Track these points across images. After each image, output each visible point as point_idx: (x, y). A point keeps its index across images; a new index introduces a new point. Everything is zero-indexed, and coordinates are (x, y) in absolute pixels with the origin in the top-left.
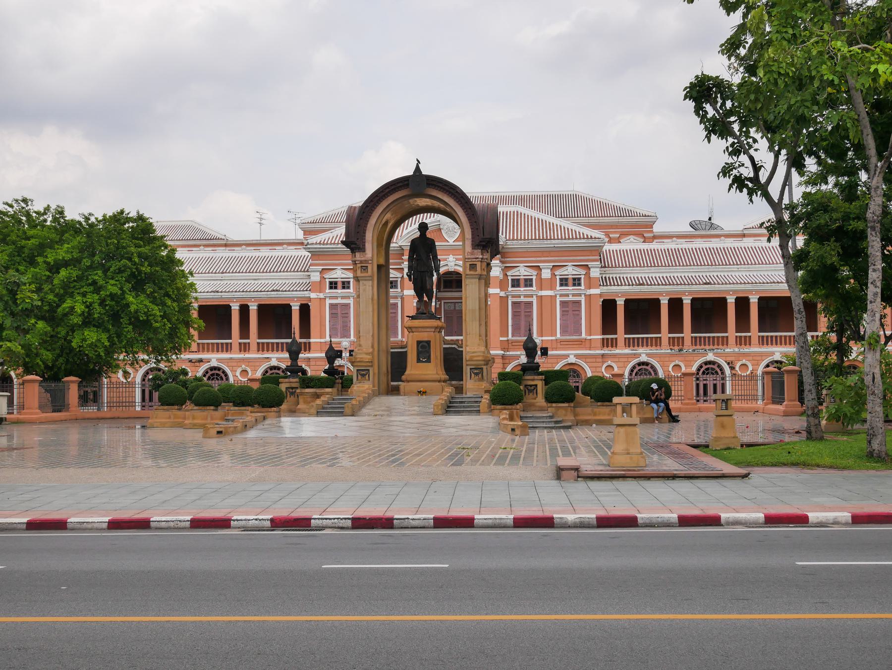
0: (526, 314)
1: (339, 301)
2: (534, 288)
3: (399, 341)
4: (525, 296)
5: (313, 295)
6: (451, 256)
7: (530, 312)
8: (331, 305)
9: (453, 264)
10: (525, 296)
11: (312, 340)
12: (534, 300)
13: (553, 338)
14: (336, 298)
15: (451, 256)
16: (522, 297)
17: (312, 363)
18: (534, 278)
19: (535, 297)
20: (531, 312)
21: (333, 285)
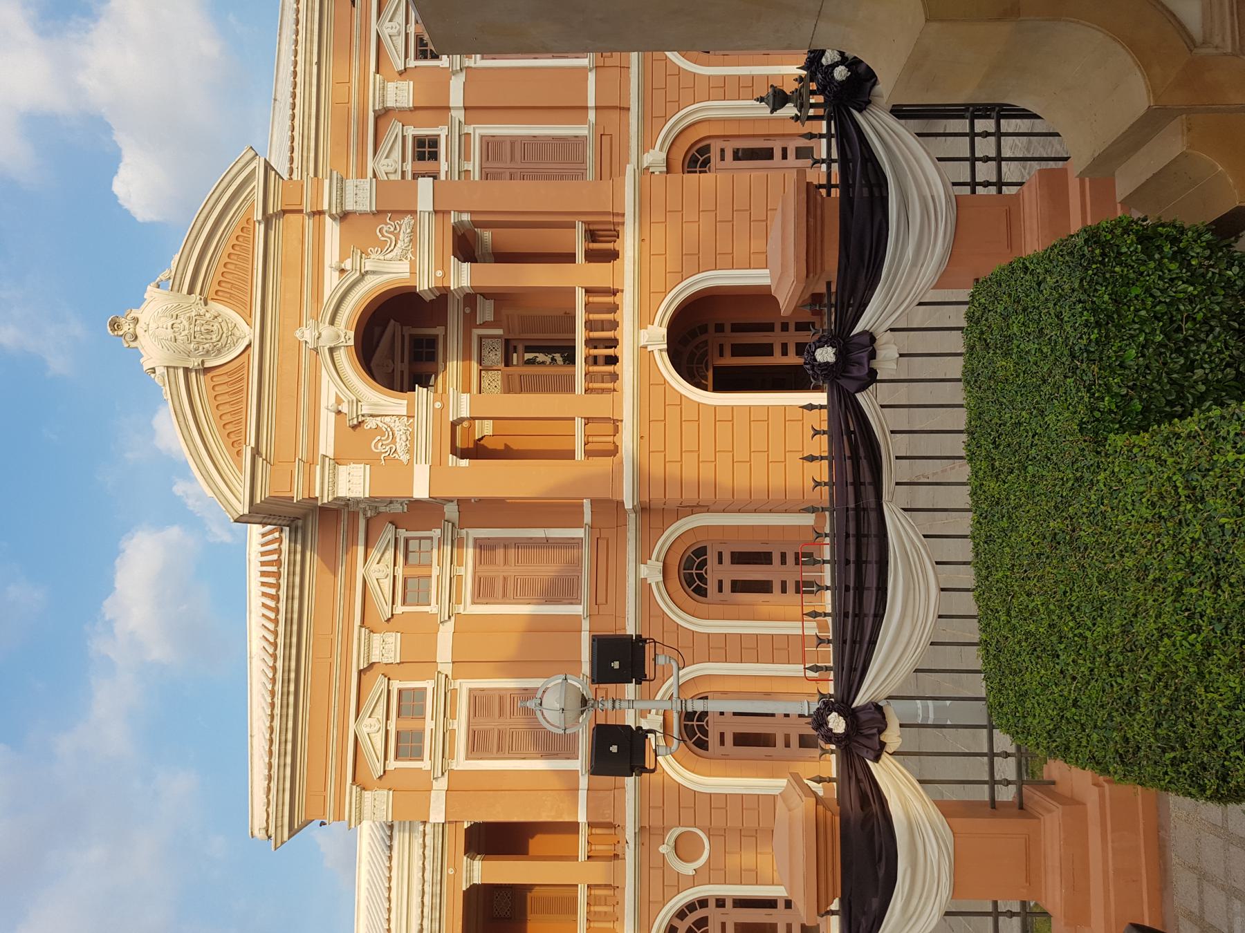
0: (518, 155)
1: (460, 725)
2: (442, 132)
3: (591, 535)
4: (465, 155)
5: (437, 815)
6: (298, 334)
7: (512, 144)
8: (477, 746)
9: (326, 331)
10: (465, 155)
11: (582, 818)
12: (479, 131)
13: (592, 77)
14: (448, 736)
15: (298, 334)
16: (468, 166)
17: (656, 821)
18: (411, 131)
19: (468, 129)
20: (513, 140)
21: (408, 745)
